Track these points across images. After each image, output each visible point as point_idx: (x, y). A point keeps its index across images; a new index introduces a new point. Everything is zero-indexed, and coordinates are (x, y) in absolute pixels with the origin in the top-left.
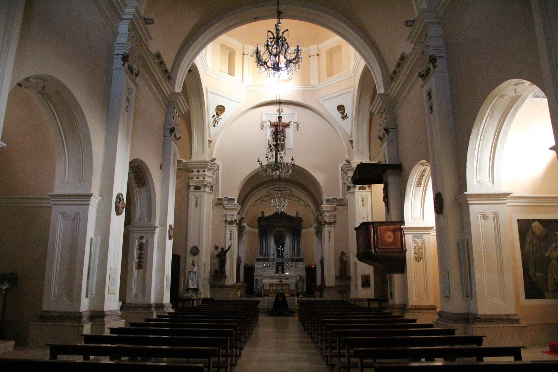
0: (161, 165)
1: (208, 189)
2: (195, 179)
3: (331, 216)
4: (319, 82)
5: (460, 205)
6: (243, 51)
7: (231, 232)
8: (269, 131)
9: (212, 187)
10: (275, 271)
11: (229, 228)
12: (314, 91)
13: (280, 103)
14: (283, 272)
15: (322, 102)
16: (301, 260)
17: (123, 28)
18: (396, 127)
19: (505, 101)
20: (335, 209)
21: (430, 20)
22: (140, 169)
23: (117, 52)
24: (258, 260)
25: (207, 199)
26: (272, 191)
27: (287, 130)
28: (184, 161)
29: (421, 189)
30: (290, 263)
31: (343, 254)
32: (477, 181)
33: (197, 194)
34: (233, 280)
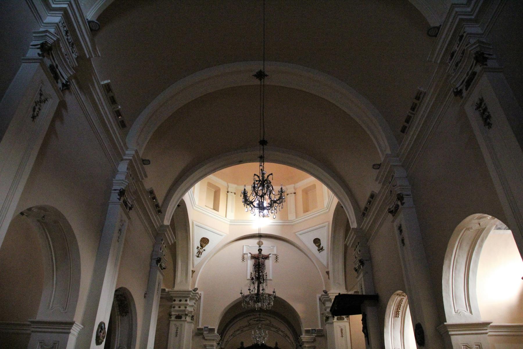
0: (145, 294)
1: (188, 319)
2: (177, 308)
4: (296, 217)
5: (442, 336)
6: (228, 189)
8: (250, 263)
9: (193, 317)
12: (292, 225)
13: (260, 236)
15: (300, 236)
17: (123, 167)
18: (370, 259)
19: (470, 234)
20: (315, 340)
21: (394, 164)
22: (125, 297)
23: (115, 187)
25: (187, 329)
26: (251, 322)
27: (267, 261)
28: (167, 290)
29: (399, 319)
32: (454, 312)
33: (178, 323)
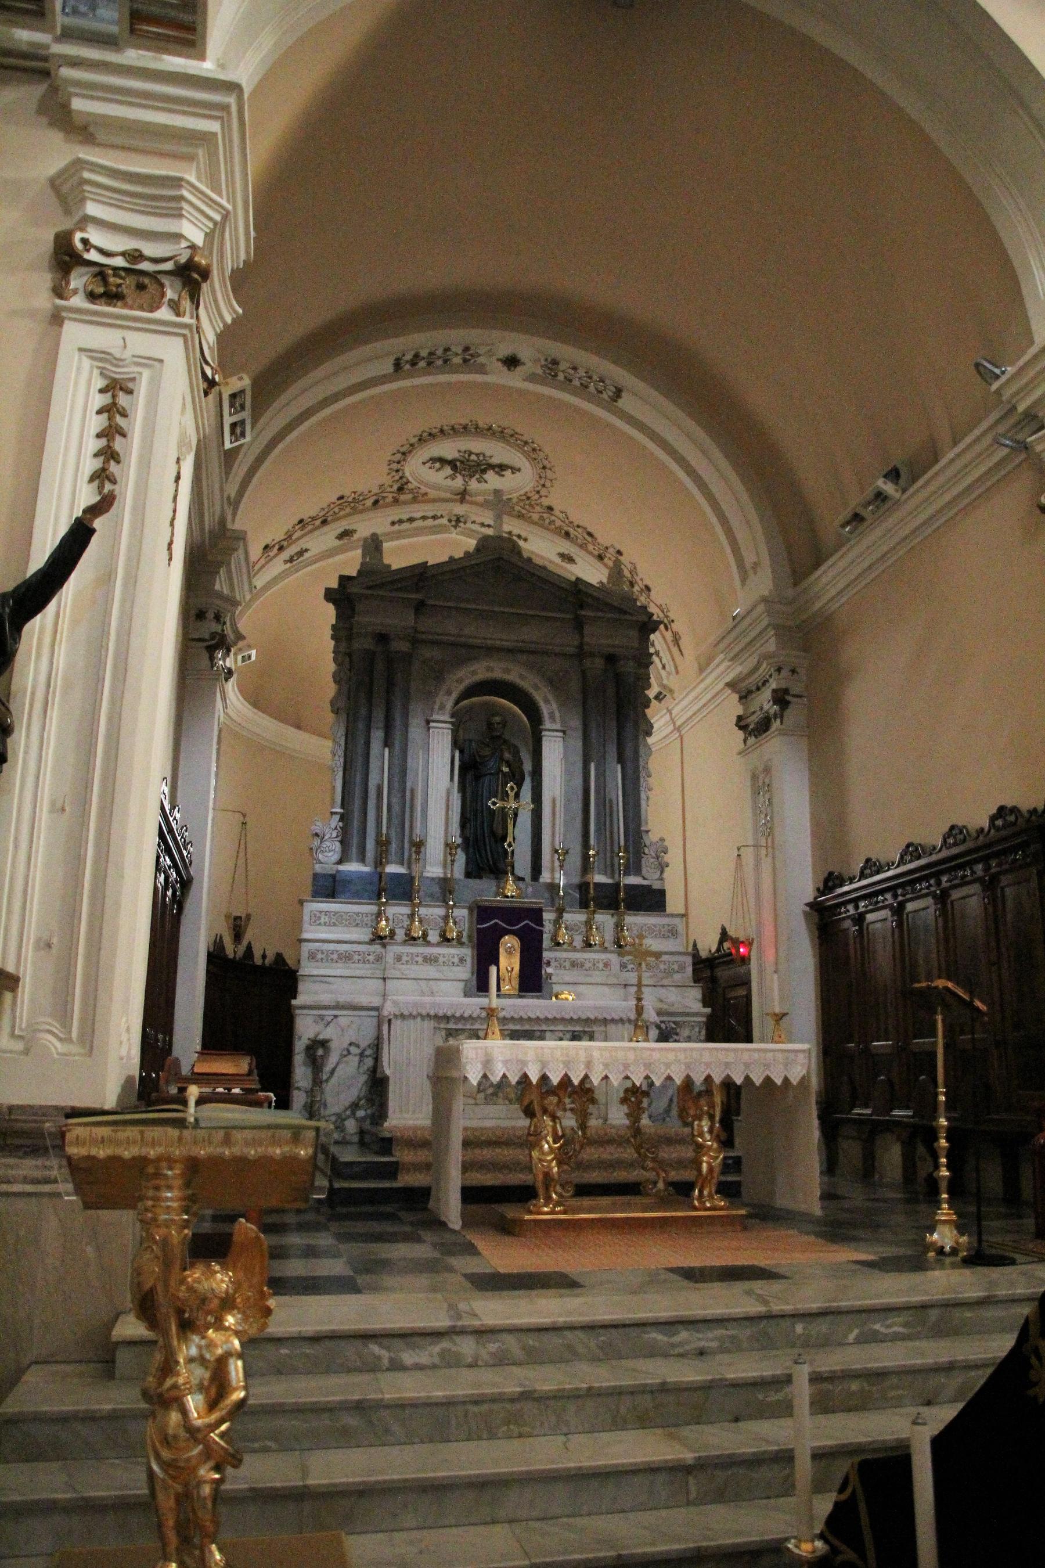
7: (116, 387)
10: (465, 972)
14: (532, 980)
16: (651, 900)
24: (329, 887)
26: (416, 469)
30: (575, 917)
34: (90, 1038)
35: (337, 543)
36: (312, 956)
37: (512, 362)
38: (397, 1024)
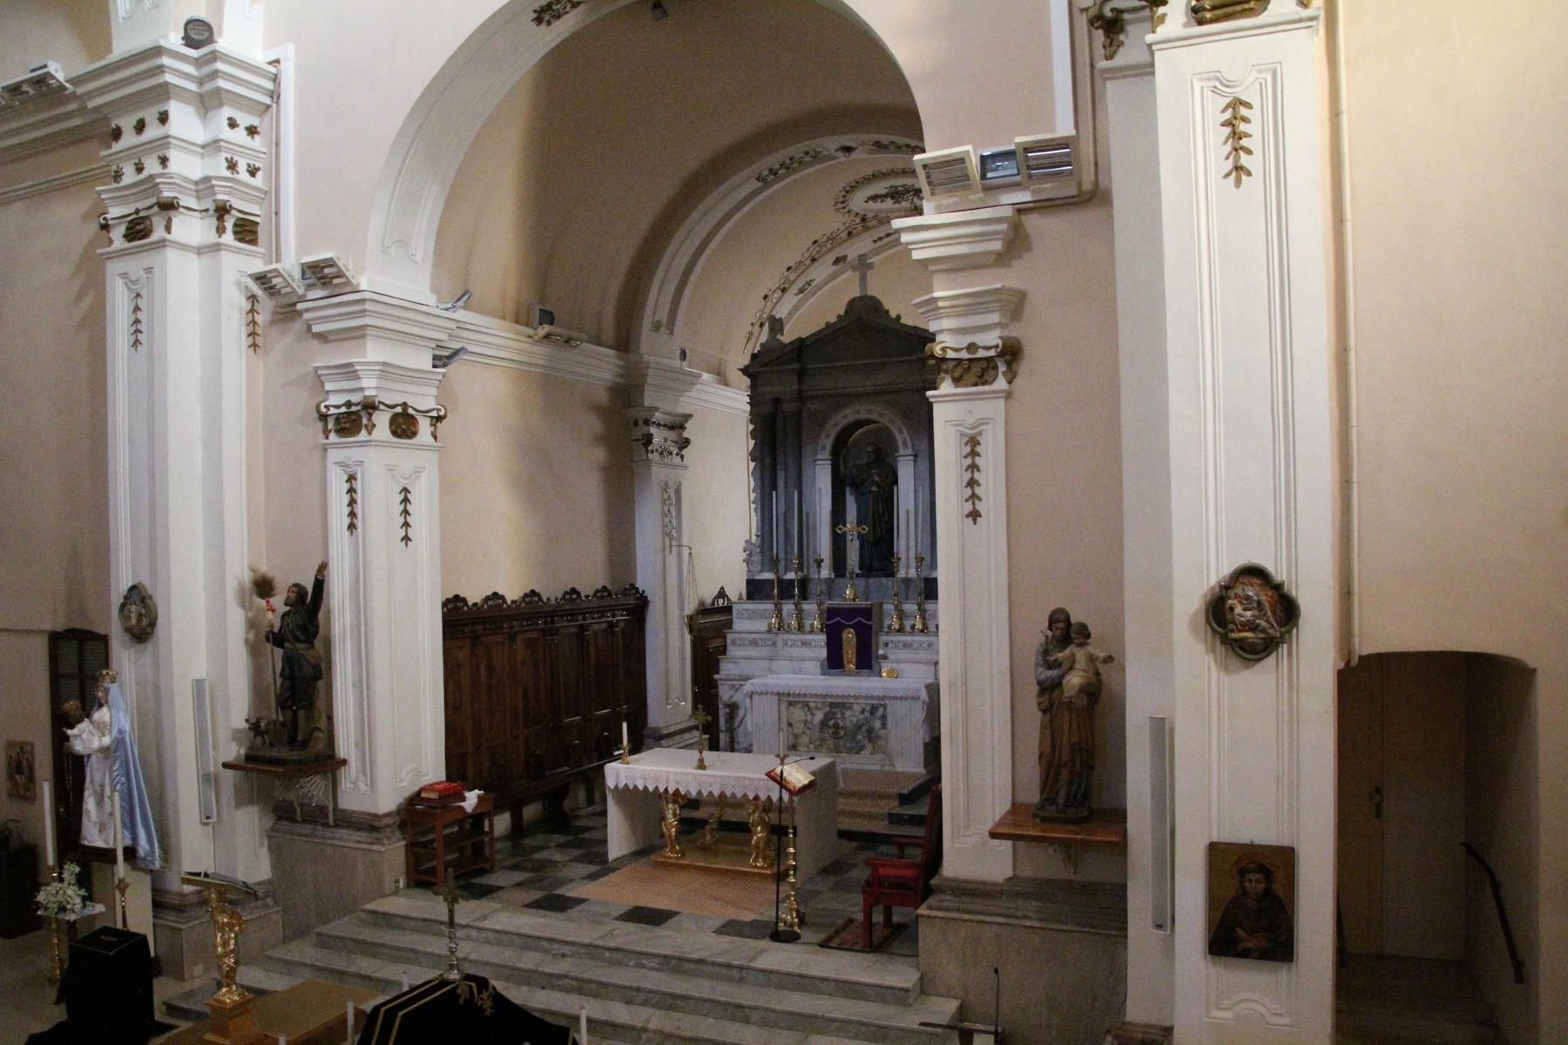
2: (129, 176)
3: (975, 304)
7: (351, 478)
10: (823, 653)
11: (342, 452)
14: (866, 661)
20: (1016, 243)
31: (1066, 631)
35: (835, 268)
36: (734, 643)
37: (848, 150)
38: (756, 698)
